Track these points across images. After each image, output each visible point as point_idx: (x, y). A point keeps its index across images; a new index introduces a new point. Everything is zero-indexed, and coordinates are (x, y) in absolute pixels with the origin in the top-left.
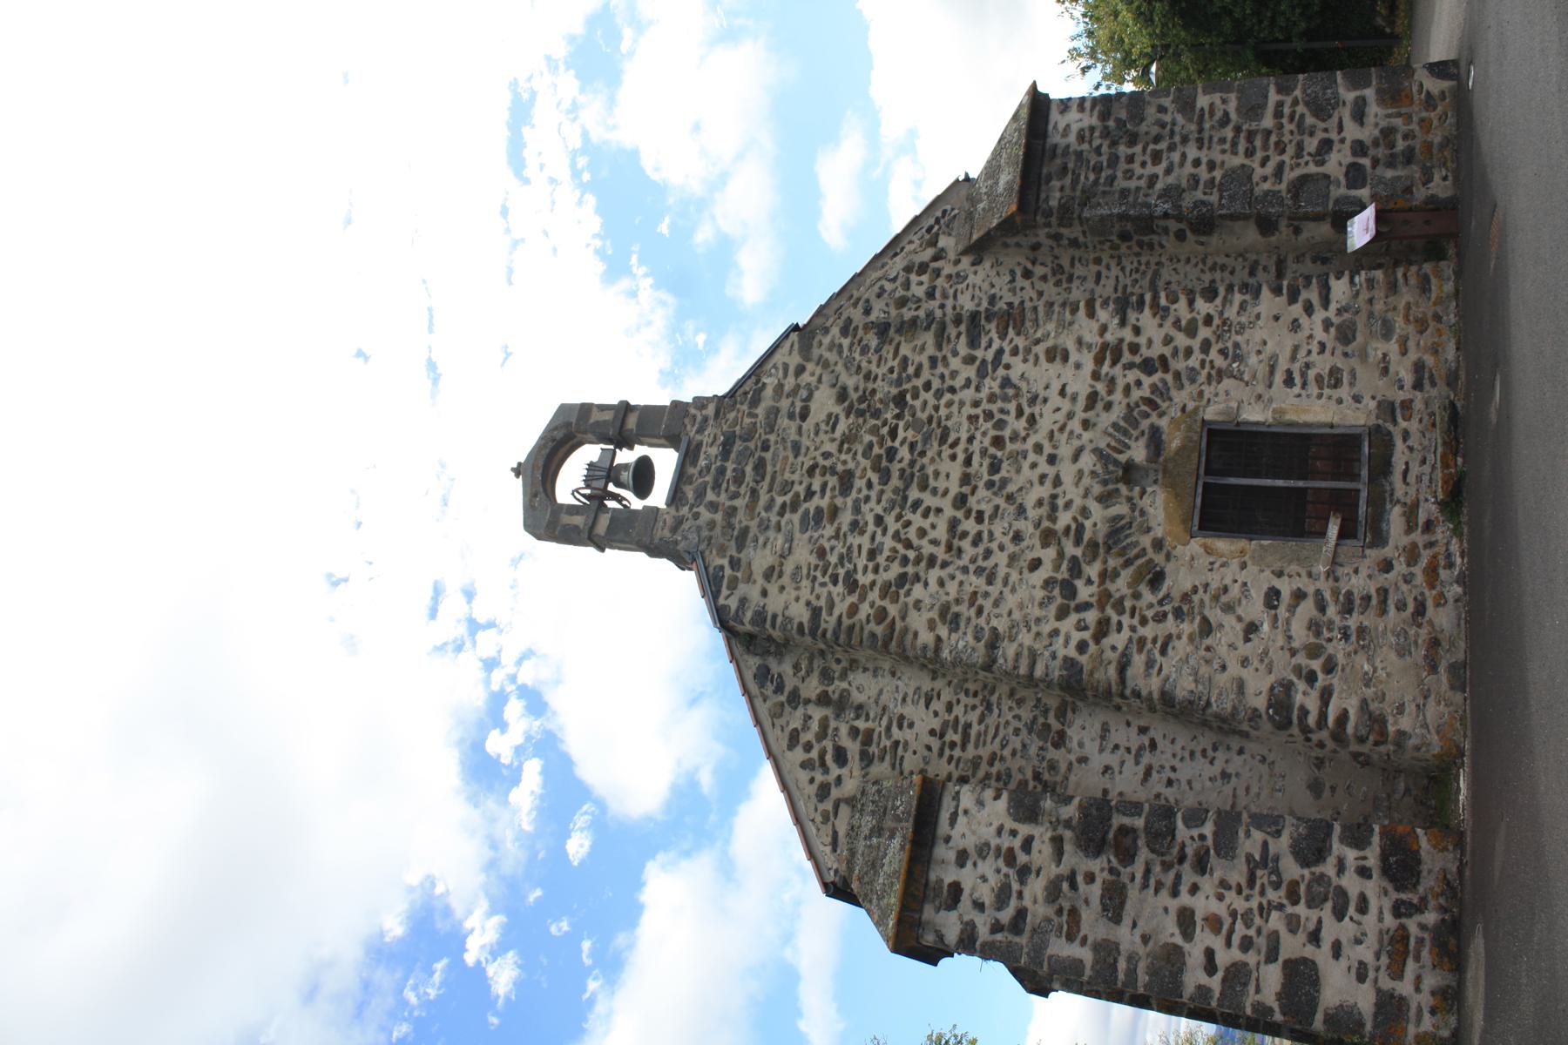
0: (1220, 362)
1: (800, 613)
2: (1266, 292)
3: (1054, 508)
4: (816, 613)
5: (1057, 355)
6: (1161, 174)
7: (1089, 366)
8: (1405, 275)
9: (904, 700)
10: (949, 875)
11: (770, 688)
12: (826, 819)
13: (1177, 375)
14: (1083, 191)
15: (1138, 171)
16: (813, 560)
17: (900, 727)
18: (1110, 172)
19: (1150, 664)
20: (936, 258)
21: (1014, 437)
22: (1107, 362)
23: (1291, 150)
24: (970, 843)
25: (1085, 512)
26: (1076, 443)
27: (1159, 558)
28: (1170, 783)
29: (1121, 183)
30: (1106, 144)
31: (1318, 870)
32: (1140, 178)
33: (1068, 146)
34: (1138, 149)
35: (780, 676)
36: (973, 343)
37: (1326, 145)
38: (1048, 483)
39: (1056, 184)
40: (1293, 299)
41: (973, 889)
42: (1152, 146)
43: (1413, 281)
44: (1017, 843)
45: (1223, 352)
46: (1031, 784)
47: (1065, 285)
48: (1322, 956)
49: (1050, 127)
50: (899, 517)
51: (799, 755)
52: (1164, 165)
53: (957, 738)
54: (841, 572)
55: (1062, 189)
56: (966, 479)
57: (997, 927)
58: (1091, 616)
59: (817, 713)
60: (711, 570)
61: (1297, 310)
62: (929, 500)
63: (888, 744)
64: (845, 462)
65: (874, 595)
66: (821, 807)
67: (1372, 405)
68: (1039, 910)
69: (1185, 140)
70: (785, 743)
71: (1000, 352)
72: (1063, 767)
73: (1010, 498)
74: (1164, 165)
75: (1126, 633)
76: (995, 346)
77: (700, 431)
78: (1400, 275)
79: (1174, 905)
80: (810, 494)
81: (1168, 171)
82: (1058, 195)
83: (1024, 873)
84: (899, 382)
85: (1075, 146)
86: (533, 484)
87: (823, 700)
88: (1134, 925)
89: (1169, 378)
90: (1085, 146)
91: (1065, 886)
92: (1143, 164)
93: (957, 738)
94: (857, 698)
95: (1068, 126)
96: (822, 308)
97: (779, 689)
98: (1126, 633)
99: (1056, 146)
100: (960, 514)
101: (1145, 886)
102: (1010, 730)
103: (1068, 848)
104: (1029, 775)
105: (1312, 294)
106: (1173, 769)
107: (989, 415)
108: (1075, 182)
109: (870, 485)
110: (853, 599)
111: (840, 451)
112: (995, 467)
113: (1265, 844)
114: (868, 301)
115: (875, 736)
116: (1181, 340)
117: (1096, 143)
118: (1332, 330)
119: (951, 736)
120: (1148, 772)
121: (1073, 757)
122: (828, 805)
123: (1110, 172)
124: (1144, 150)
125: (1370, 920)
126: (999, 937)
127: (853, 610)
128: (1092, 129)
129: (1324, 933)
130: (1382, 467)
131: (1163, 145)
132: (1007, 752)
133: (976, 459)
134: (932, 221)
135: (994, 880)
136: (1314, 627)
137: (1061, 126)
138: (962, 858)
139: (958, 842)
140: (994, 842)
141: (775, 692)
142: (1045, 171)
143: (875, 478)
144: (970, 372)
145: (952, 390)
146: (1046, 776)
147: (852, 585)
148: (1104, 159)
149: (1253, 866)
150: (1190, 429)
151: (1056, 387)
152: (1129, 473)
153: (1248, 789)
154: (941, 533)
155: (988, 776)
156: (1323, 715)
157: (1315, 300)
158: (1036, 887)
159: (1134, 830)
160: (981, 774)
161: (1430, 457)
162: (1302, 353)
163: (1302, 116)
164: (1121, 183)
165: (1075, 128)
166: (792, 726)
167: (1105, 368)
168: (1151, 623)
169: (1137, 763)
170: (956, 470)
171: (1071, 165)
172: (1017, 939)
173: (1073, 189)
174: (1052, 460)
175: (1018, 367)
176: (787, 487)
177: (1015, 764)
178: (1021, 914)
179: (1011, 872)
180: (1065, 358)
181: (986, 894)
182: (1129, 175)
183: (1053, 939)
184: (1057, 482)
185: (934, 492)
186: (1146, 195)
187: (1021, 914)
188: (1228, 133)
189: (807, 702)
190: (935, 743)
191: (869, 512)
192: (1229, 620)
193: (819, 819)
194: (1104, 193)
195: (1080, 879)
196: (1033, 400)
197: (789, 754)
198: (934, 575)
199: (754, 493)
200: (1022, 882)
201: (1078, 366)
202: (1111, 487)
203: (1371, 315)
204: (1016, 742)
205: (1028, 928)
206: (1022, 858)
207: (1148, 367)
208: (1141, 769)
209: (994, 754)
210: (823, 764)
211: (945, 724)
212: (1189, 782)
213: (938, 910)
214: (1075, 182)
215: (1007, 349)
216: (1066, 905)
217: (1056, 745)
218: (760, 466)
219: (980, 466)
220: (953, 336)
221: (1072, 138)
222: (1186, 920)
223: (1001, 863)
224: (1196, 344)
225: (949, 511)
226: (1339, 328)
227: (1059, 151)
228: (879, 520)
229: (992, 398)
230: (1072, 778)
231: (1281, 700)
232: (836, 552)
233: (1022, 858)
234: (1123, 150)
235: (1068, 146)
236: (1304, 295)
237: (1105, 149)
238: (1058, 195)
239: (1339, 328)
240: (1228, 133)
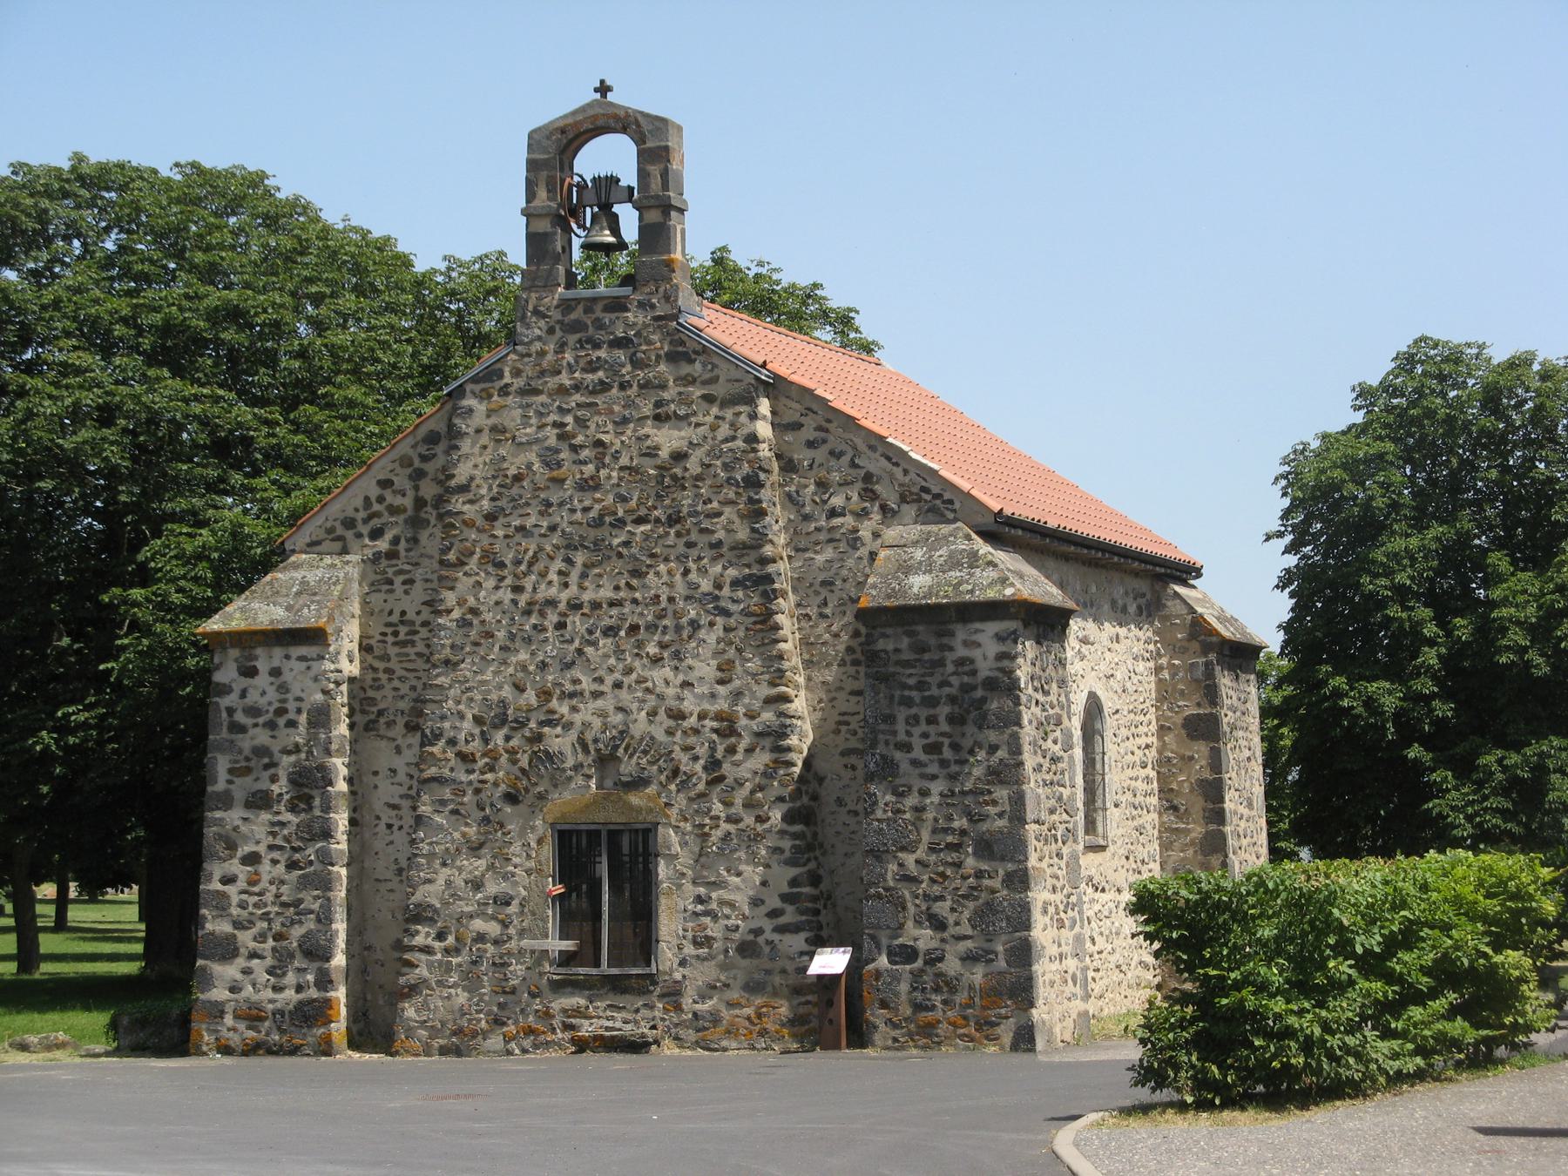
0: (717, 834)
1: (462, 473)
2: (793, 872)
3: (572, 695)
4: (464, 489)
5: (725, 673)
6: (913, 755)
7: (712, 708)
8: (808, 1003)
9: (427, 581)
10: (262, 665)
11: (422, 449)
12: (330, 531)
13: (702, 795)
14: (894, 674)
15: (917, 731)
16: (512, 471)
17: (404, 583)
18: (918, 700)
19: (443, 803)
20: (884, 508)
21: (640, 645)
22: (715, 724)
23: (937, 890)
24: (287, 676)
25: (568, 726)
26: (634, 706)
27: (529, 799)
28: (389, 826)
29: (902, 714)
30: (953, 691)
31: (298, 955)
32: (908, 733)
33: (951, 649)
34: (945, 727)
35: (434, 455)
36: (736, 583)
37: (939, 925)
38: (595, 687)
39: (905, 642)
40: (785, 898)
41: (255, 687)
42: (946, 741)
43: (801, 1010)
44: (292, 715)
45: (727, 837)
46: (375, 709)
47: (848, 659)
48: (241, 962)
49: (978, 625)
50: (557, 547)
51: (374, 492)
52: (923, 757)
53: (402, 637)
54: (502, 503)
55: (897, 650)
56: (596, 605)
57: (231, 711)
58: (476, 746)
59: (408, 502)
60: (498, 366)
61: (775, 903)
62: (574, 577)
63: (390, 575)
64: (609, 477)
65: (485, 541)
66: (337, 524)
67: (678, 976)
68: (246, 743)
69: (953, 777)
70: (381, 477)
71: (726, 613)
72: (390, 734)
73: (580, 652)
74: (923, 757)
75: (464, 778)
76: (733, 608)
77: (641, 305)
78: (810, 998)
79: (261, 849)
80: (575, 449)
81: (915, 763)
82: (890, 647)
83: (271, 725)
84: (695, 514)
85: (950, 657)
86: (576, 123)
87: (420, 503)
88: (245, 819)
89: (701, 787)
90: (950, 668)
91: (266, 760)
92: (925, 735)
93: (402, 637)
94: (424, 536)
95: (979, 645)
96: (810, 392)
97: (424, 458)
98: (464, 778)
99: (952, 634)
100: (562, 606)
101: (273, 824)
102: (414, 682)
103: (293, 758)
104: (382, 706)
105: (790, 916)
106: (401, 828)
107: (661, 616)
108: (907, 664)
109: (586, 510)
110: (480, 522)
111: (622, 469)
112: (610, 631)
113: (312, 912)
114: (824, 441)
115: (394, 562)
116: (739, 797)
117: (954, 680)
118: (751, 937)
119: (403, 630)
120: (395, 807)
121: (399, 741)
122: (340, 531)
123: (918, 700)
124: (943, 734)
125: (269, 994)
126: (224, 715)
127: (469, 524)
128: (974, 673)
129: (256, 961)
130: (617, 985)
131: (947, 753)
132: (396, 683)
133: (614, 611)
134: (936, 490)
135: (262, 701)
136: (481, 938)
137: (978, 638)
138: (276, 672)
139: (286, 666)
140: (290, 696)
141: (420, 456)
142: (920, 628)
143: (593, 514)
144: (706, 585)
145: (686, 572)
146: (382, 720)
147: (491, 517)
148: (935, 691)
149: (297, 903)
150: (651, 810)
151: (692, 677)
152: (605, 761)
153: (391, 891)
154: (544, 592)
155: (375, 670)
156: (411, 949)
157: (782, 920)
158: (262, 737)
159: (311, 808)
160: (377, 664)
161: (629, 1027)
162: (727, 911)
163: (976, 898)
164: (902, 714)
165: (976, 654)
166: (395, 479)
167: (709, 723)
168: (476, 798)
169: (401, 797)
170: (606, 593)
171: (926, 656)
172: (225, 729)
173: (898, 663)
174: (618, 685)
175: (711, 637)
176: (581, 423)
177: (388, 691)
178: (242, 729)
179: (270, 715)
180: (721, 682)
181: (253, 697)
182: (913, 720)
183: (228, 757)
184: (597, 695)
185: (584, 576)
186: (887, 743)
187: (242, 729)
188: (960, 823)
189: (417, 488)
190: (395, 618)
191: (562, 518)
192: (482, 864)
193: (329, 525)
194: (892, 697)
195: (272, 771)
196: (677, 655)
197: (374, 482)
198: (507, 596)
199: (577, 387)
200: (265, 725)
201: (713, 696)
202: (592, 748)
203: (768, 972)
204: (405, 689)
205: (233, 736)
206: (281, 721)
207: (713, 764)
208: (396, 801)
209: (394, 672)
210: (370, 517)
211: (412, 623)
212: (392, 842)
213: (236, 660)
214: (907, 664)
215: (732, 622)
216: (252, 764)
217: (407, 725)
218: (604, 387)
219: (609, 617)
220: (745, 560)
221: (961, 652)
222: (252, 859)
223: (277, 705)
224: (738, 808)
225: (564, 596)
226: (754, 943)
227: (945, 640)
228: (553, 528)
229: (677, 615)
230: (384, 743)
231: (420, 915)
232: (521, 491)
233: (281, 721)
234: (944, 711)
235: (951, 649)
236: (790, 909)
237: (947, 690)
238: (890, 647)
239: (754, 943)
240: (960, 823)
